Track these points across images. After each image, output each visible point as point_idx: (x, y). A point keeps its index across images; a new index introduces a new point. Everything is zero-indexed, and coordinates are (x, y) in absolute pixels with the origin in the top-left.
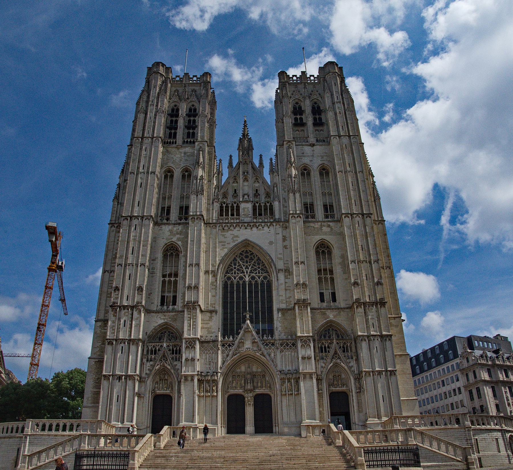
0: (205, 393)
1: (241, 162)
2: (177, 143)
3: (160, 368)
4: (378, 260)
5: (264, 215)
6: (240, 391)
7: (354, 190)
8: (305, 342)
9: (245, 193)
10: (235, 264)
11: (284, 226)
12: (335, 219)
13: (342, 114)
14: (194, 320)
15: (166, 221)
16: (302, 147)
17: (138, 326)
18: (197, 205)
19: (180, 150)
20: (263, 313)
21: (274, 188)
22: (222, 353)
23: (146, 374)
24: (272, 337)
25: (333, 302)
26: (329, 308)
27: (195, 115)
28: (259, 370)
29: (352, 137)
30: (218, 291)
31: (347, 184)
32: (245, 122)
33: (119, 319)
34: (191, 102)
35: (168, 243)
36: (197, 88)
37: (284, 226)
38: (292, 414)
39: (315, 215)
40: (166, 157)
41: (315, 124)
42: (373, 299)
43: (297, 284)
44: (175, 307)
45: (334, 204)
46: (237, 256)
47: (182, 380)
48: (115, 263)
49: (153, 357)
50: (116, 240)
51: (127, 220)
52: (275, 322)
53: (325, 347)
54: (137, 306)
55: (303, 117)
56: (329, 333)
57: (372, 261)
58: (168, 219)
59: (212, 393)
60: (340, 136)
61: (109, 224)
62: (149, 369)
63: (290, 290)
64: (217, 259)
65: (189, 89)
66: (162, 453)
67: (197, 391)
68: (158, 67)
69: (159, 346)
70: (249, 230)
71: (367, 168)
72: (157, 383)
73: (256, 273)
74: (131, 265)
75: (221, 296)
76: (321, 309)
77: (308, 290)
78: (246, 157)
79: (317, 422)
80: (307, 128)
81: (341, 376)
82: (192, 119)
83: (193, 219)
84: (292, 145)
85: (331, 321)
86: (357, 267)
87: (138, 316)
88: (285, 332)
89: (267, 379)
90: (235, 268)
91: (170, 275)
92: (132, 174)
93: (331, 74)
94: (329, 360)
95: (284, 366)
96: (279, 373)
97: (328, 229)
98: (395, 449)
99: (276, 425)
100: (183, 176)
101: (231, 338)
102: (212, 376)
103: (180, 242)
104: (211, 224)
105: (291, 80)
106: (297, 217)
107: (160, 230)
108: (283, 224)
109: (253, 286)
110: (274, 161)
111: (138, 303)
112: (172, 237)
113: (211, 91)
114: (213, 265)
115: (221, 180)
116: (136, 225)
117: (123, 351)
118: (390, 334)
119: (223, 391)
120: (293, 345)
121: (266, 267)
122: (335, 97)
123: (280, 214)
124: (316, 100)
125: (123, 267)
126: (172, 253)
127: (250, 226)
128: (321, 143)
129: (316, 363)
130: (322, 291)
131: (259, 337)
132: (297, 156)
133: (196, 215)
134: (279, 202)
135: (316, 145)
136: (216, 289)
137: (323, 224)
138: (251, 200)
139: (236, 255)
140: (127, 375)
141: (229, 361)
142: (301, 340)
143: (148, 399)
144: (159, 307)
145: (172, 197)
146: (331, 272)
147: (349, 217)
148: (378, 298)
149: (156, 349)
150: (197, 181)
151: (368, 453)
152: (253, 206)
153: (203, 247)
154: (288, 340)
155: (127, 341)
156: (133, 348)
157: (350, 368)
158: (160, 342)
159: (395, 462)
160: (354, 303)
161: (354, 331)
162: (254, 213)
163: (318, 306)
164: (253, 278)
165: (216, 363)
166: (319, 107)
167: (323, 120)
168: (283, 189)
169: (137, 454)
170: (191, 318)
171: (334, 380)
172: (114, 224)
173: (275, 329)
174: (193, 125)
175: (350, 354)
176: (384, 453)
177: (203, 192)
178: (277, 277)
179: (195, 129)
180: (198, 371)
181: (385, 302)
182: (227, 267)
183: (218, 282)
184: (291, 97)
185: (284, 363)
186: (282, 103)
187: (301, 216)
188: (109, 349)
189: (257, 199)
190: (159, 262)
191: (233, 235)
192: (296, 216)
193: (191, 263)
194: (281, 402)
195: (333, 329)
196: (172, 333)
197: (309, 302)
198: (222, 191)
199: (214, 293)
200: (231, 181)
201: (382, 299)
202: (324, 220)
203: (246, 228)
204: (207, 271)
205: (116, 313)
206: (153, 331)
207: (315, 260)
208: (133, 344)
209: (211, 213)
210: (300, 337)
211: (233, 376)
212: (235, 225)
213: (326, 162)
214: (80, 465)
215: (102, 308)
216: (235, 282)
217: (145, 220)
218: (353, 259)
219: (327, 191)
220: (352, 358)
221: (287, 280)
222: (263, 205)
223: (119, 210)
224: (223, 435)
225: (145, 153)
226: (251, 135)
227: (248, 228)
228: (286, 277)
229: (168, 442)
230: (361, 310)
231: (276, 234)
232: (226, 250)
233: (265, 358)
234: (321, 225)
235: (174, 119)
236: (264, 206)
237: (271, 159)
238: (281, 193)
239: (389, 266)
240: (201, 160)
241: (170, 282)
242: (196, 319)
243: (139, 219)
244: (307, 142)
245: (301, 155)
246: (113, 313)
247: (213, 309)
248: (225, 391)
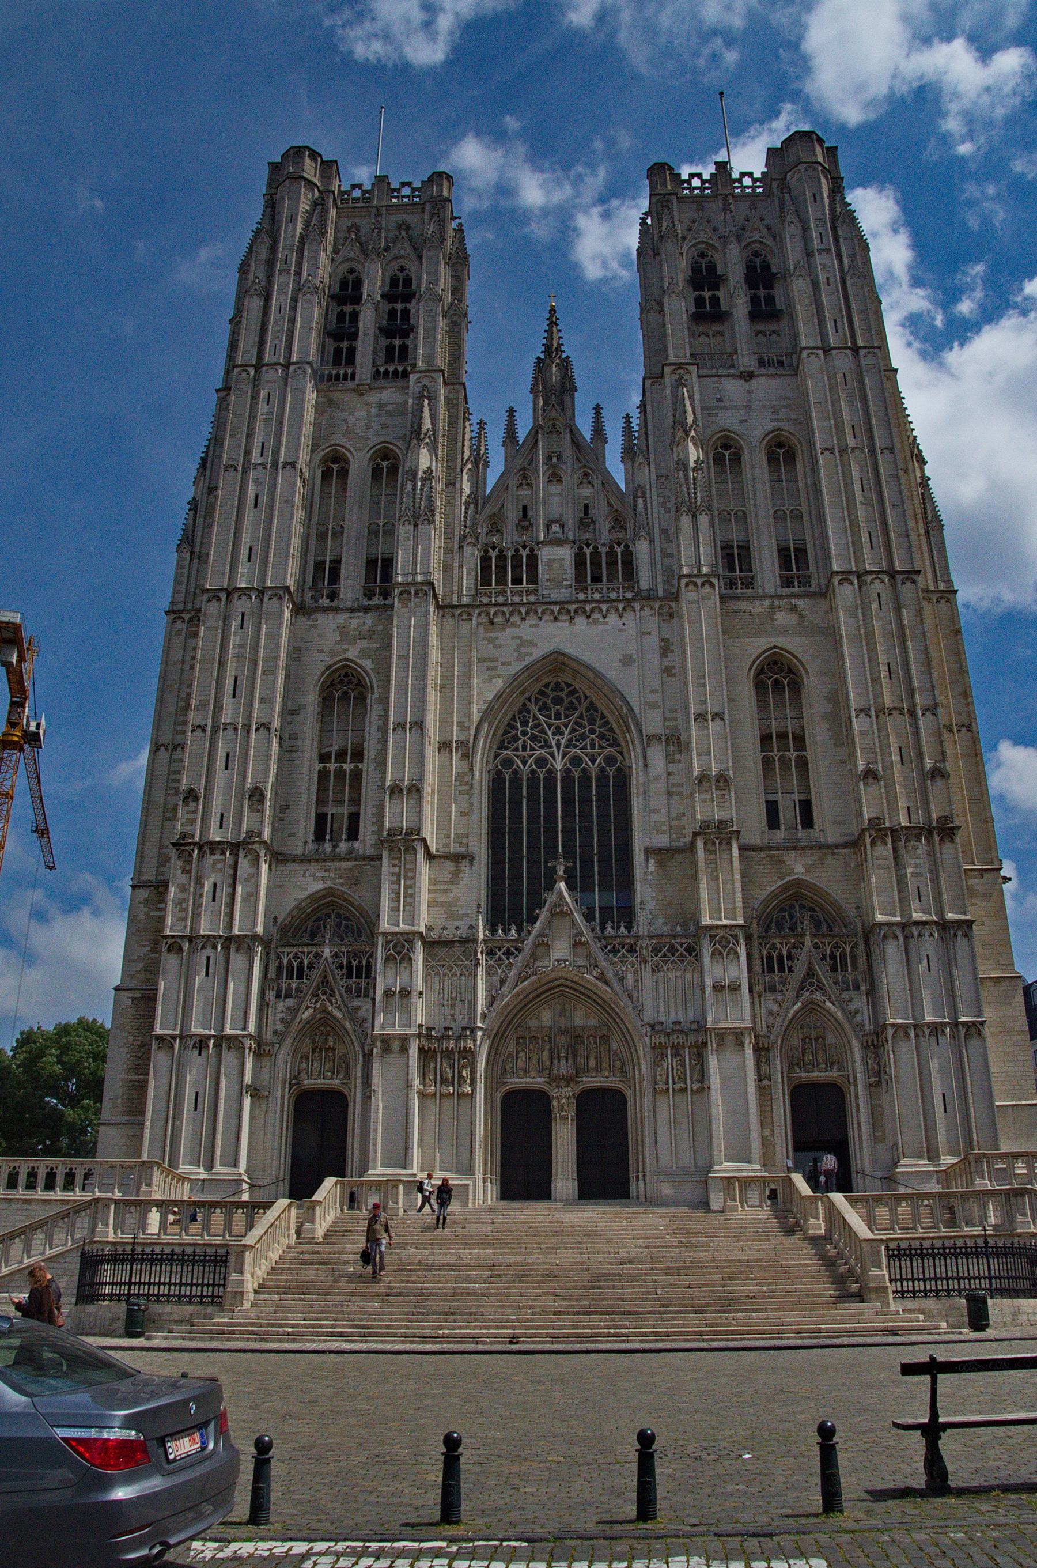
0: (438, 1085)
1: (542, 427)
2: (357, 378)
3: (313, 1016)
4: (936, 705)
5: (608, 580)
6: (536, 1081)
7: (867, 503)
8: (724, 942)
9: (551, 517)
10: (525, 723)
11: (666, 610)
12: (812, 589)
13: (832, 286)
14: (409, 882)
15: (328, 601)
16: (717, 382)
17: (253, 899)
18: (415, 555)
19: (365, 398)
20: (605, 861)
21: (635, 501)
22: (488, 974)
23: (275, 1032)
24: (629, 928)
25: (803, 828)
26: (795, 847)
27: (408, 297)
28: (593, 1022)
29: (862, 352)
30: (475, 801)
31: (848, 484)
32: (553, 311)
33: (199, 882)
34: (396, 258)
35: (336, 663)
36: (412, 219)
37: (666, 610)
38: (685, 1145)
39: (752, 578)
40: (324, 420)
41: (755, 316)
42: (919, 820)
43: (702, 778)
44: (356, 844)
45: (809, 546)
46: (529, 699)
47: (375, 1050)
48: (186, 723)
49: (294, 986)
50: (188, 658)
51: (219, 599)
52: (638, 886)
53: (780, 958)
54: (249, 843)
55: (720, 294)
56: (791, 916)
57: (919, 708)
58: (333, 596)
59: (460, 1086)
60: (827, 350)
61: (167, 613)
62: (282, 1020)
63: (680, 794)
64: (475, 708)
65: (389, 222)
66: (318, 1253)
67: (417, 1082)
68: (300, 160)
69: (312, 955)
70: (563, 625)
71: (905, 438)
72: (305, 1057)
73: (585, 747)
74: (230, 728)
75: (485, 814)
76: (770, 848)
77: (732, 794)
78: (554, 414)
79: (754, 1169)
80: (733, 326)
81: (824, 1039)
82: (399, 306)
83: (405, 596)
84: (687, 376)
85: (799, 883)
86: (875, 726)
87: (251, 871)
88: (665, 916)
89: (615, 1046)
90: (525, 733)
91: (341, 756)
92: (231, 470)
93: (802, 167)
94: (790, 994)
95: (662, 1010)
96: (649, 1029)
97: (793, 618)
98: (976, 1248)
99: (637, 1177)
100: (377, 472)
101: (513, 931)
102: (458, 1039)
103: (370, 661)
104: (456, 607)
105: (686, 188)
106: (703, 584)
107: (311, 626)
108: (660, 608)
110: (635, 423)
111: (250, 834)
112: (346, 647)
113: (454, 224)
114: (462, 726)
115: (485, 479)
116: (243, 614)
117: (211, 970)
118: (968, 917)
119: (489, 1080)
120: (690, 950)
121: (611, 730)
122: (815, 236)
123: (653, 577)
124: (758, 245)
125: (208, 733)
126: (346, 693)
127: (569, 612)
128: (772, 371)
129: (752, 1004)
130: (772, 797)
131: (593, 930)
132: (703, 408)
133: (414, 583)
134: (652, 541)
135: (758, 376)
136: (469, 793)
137: (777, 602)
138: (571, 537)
139: (527, 694)
140: (222, 1037)
141: (507, 997)
142: (712, 937)
143: (281, 1099)
144: (311, 846)
145: (346, 531)
146: (800, 741)
147: (851, 583)
148: (935, 815)
149: (302, 963)
150: (415, 485)
151: (899, 1257)
152: (576, 554)
153: (434, 673)
154: (675, 937)
155: (221, 941)
156: (238, 960)
157: (851, 1015)
158: (315, 945)
159: (975, 1284)
160: (863, 830)
161: (863, 910)
163: (761, 840)
164: (576, 761)
165: (470, 1003)
166: (766, 266)
167: (777, 302)
168: (663, 504)
169: (248, 1256)
170: (398, 876)
171: (804, 1049)
172: (182, 612)
173: (638, 907)
174: (401, 324)
175: (850, 978)
176: (945, 1259)
177: (433, 515)
178: (645, 758)
179: (408, 337)
180: (420, 1026)
181: (954, 828)
182: (500, 732)
183: (477, 773)
184: (684, 238)
185: (662, 1004)
186: (659, 254)
187: (714, 580)
188: (170, 963)
189: (588, 535)
190: (310, 719)
191: (516, 638)
192: (699, 581)
193: (401, 720)
194: (654, 1111)
195: (802, 907)
196: (347, 919)
197: (735, 828)
198: (488, 511)
199: (466, 805)
200: (513, 483)
201: (946, 817)
202: (780, 591)
203: (556, 619)
204: (444, 743)
205: (190, 862)
206: (295, 913)
207: (755, 708)
208: (237, 950)
209: (456, 576)
210: (708, 928)
211: (518, 1038)
212: (523, 610)
214: (93, 1284)
215: (151, 851)
216: (525, 772)
217: (270, 599)
218: (863, 704)
219: (787, 508)
220: (857, 988)
221: (672, 767)
222: (603, 551)
223: (194, 573)
224: (489, 1202)
226: (568, 351)
227: (562, 617)
228: (669, 758)
229: (335, 1222)
230: (885, 850)
231: (643, 633)
232: (499, 684)
233: (608, 989)
234: (772, 607)
235: (348, 309)
236: (607, 553)
237: (628, 418)
238: (655, 515)
239: (967, 722)
241: (340, 774)
242: (413, 878)
243: (251, 598)
244: (733, 366)
245: (717, 404)
246: (180, 863)
247: (463, 849)
248: (495, 1081)
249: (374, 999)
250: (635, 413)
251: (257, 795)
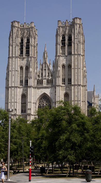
10: (41, 100)
41: (68, 46)
48: (8, 101)
58: (22, 85)
91: (24, 103)
100: (26, 69)
110: (54, 62)
128: (69, 55)
162: (47, 83)
164: (46, 104)
213: (70, 63)
219: (70, 74)
225: (14, 63)
232: (39, 96)
234: (67, 87)
237: (53, 61)
240: (31, 65)
241: (24, 105)
244: (65, 54)
250: (54, 60)
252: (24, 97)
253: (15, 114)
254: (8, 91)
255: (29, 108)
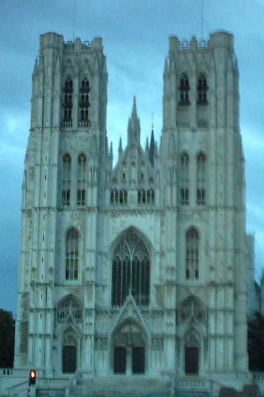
10: (122, 247)
32: (135, 97)
33: (37, 293)
58: (68, 204)
90: (122, 249)
91: (72, 253)
100: (80, 161)
109: (136, 264)
134: (160, 190)
146: (197, 252)
164: (136, 258)
166: (205, 81)
226: (140, 114)
249: (83, 325)
251: (51, 269)
252: (73, 237)
253: (51, 282)
254: (29, 220)
255: (90, 268)
